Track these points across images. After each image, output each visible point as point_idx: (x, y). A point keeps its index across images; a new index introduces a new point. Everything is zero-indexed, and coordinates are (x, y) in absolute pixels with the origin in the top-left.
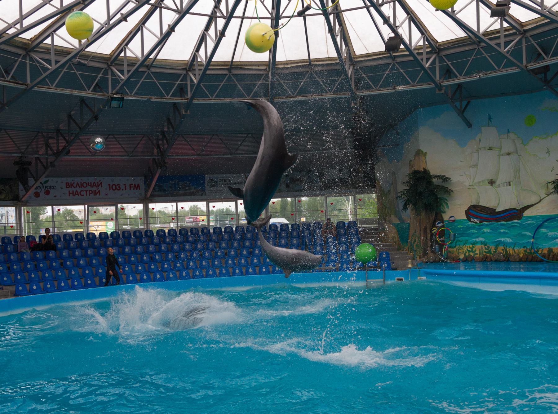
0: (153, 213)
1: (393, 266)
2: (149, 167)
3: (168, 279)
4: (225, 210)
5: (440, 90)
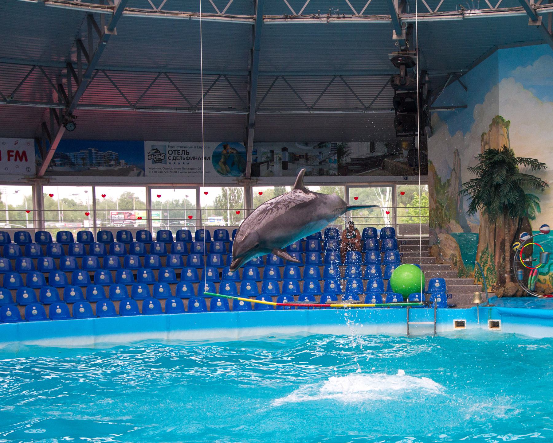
0: (52, 203)
1: (449, 301)
2: (44, 124)
3: (76, 315)
4: (181, 202)
5: (535, 20)
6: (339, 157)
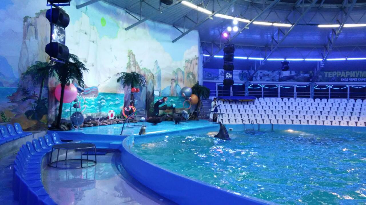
6: (279, 75)
